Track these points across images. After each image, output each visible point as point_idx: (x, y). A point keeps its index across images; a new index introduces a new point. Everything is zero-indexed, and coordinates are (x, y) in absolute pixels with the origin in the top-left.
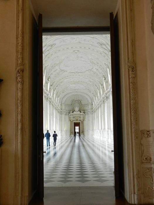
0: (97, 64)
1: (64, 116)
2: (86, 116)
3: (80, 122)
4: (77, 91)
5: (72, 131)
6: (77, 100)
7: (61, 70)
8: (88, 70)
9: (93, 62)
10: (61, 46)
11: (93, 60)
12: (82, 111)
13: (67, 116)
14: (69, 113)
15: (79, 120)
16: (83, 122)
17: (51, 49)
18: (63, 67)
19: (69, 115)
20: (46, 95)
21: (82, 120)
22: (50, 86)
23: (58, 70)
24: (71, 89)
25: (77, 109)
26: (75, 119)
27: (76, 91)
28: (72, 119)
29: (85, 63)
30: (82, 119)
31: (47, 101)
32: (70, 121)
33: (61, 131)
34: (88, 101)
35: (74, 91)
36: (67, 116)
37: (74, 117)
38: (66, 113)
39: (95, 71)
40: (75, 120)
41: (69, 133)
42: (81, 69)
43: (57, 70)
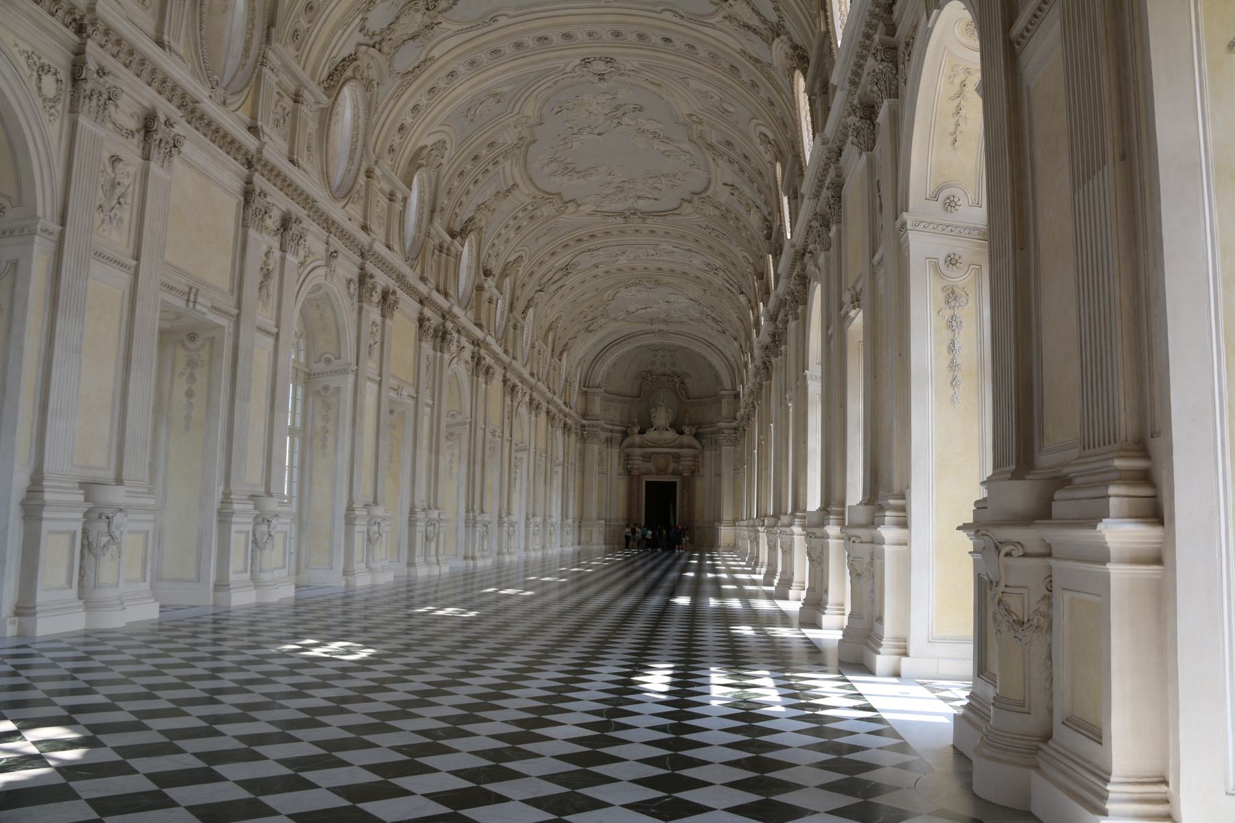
0: (725, 149)
3: (676, 482)
4: (663, 327)
6: (664, 375)
7: (538, 189)
8: (688, 197)
9: (701, 137)
10: (494, 19)
11: (701, 123)
17: (430, 27)
18: (552, 174)
20: (428, 312)
22: (477, 273)
23: (522, 186)
24: (628, 313)
25: (662, 417)
27: (656, 327)
28: (638, 463)
29: (663, 147)
31: (442, 351)
32: (629, 472)
33: (581, 521)
35: (648, 327)
36: (615, 451)
37: (647, 458)
38: (609, 434)
39: (724, 196)
40: (653, 470)
42: (657, 196)
43: (515, 186)
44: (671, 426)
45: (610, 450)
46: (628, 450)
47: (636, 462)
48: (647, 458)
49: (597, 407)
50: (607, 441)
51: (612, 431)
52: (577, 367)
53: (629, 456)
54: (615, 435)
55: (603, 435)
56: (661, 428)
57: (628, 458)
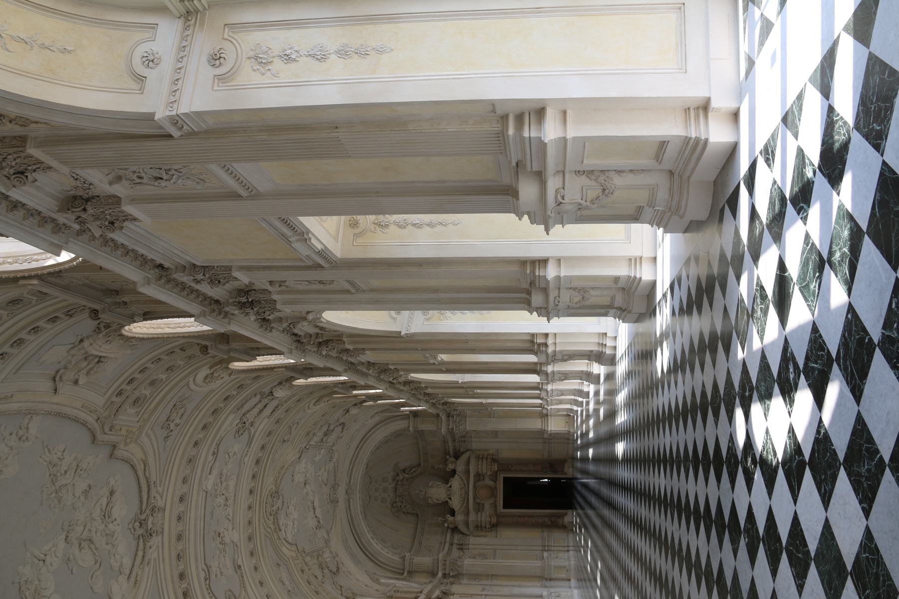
1: (467, 562)
2: (474, 446)
5: (547, 519)
12: (451, 467)
13: (473, 541)
14: (455, 530)
15: (491, 483)
16: (505, 465)
19: (467, 533)
21: (496, 468)
25: (437, 492)
26: (487, 505)
28: (485, 517)
30: (486, 468)
32: (494, 526)
34: (398, 434)
36: (472, 540)
37: (479, 508)
38: (455, 547)
40: (492, 501)
41: (558, 536)
44: (447, 481)
45: (471, 546)
46: (471, 527)
47: (483, 519)
48: (479, 508)
49: (425, 560)
50: (461, 549)
51: (452, 544)
52: (380, 584)
53: (477, 527)
54: (455, 541)
55: (455, 553)
56: (449, 492)
57: (479, 527)
